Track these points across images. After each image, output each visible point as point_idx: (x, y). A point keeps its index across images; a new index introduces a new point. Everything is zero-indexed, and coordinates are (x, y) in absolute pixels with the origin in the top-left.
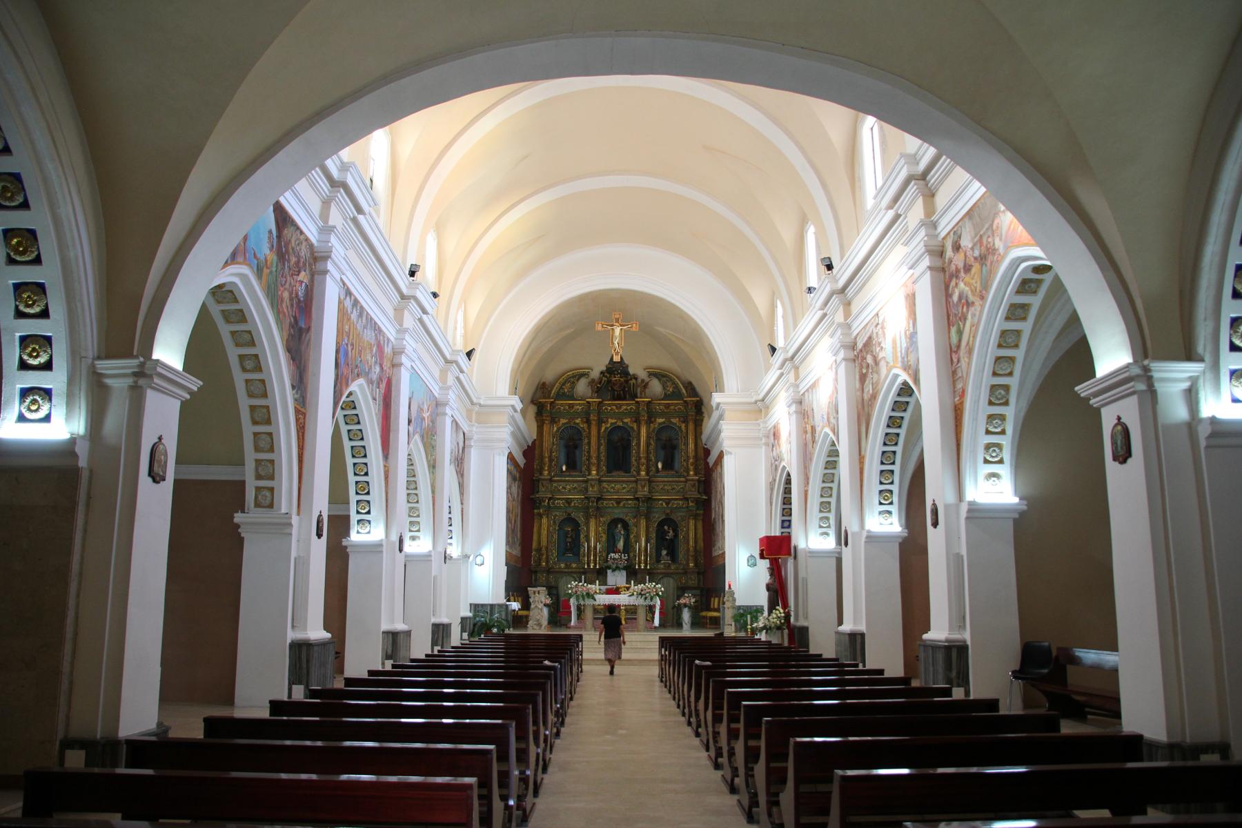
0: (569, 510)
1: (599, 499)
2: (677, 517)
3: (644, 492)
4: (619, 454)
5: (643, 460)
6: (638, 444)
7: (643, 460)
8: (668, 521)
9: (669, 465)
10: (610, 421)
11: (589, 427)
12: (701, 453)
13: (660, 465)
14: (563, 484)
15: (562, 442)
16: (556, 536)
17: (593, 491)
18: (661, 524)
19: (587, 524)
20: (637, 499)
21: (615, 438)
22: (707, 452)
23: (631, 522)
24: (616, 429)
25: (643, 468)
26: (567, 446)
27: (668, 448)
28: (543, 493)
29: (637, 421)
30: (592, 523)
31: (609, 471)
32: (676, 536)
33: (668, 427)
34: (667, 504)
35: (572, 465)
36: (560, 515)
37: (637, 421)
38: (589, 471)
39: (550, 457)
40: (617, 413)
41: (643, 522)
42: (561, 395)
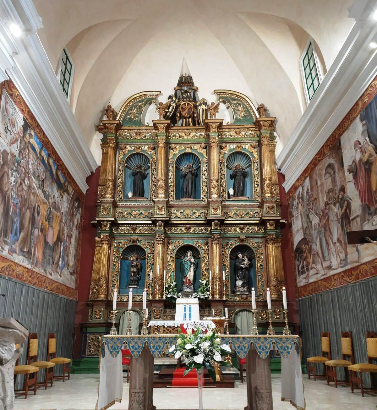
0: (135, 237)
1: (168, 224)
2: (252, 243)
3: (215, 213)
4: (188, 182)
5: (215, 183)
6: (208, 170)
7: (215, 183)
8: (242, 248)
9: (240, 191)
10: (178, 146)
11: (157, 154)
12: (275, 178)
13: (231, 192)
14: (129, 210)
15: (129, 172)
16: (118, 265)
17: (161, 214)
18: (235, 250)
19: (153, 252)
20: (208, 223)
21: (184, 167)
22: (282, 177)
23: (201, 252)
24: (185, 156)
25: (214, 191)
26: (134, 174)
27: (239, 178)
28: (105, 216)
29: (208, 147)
30: (159, 249)
31: (178, 197)
32: (251, 266)
33: (239, 153)
34: (242, 229)
35: (139, 192)
36: (124, 243)
37: (208, 147)
38: (156, 193)
39: (114, 182)
40: (186, 139)
41: (216, 248)
42: (128, 121)
